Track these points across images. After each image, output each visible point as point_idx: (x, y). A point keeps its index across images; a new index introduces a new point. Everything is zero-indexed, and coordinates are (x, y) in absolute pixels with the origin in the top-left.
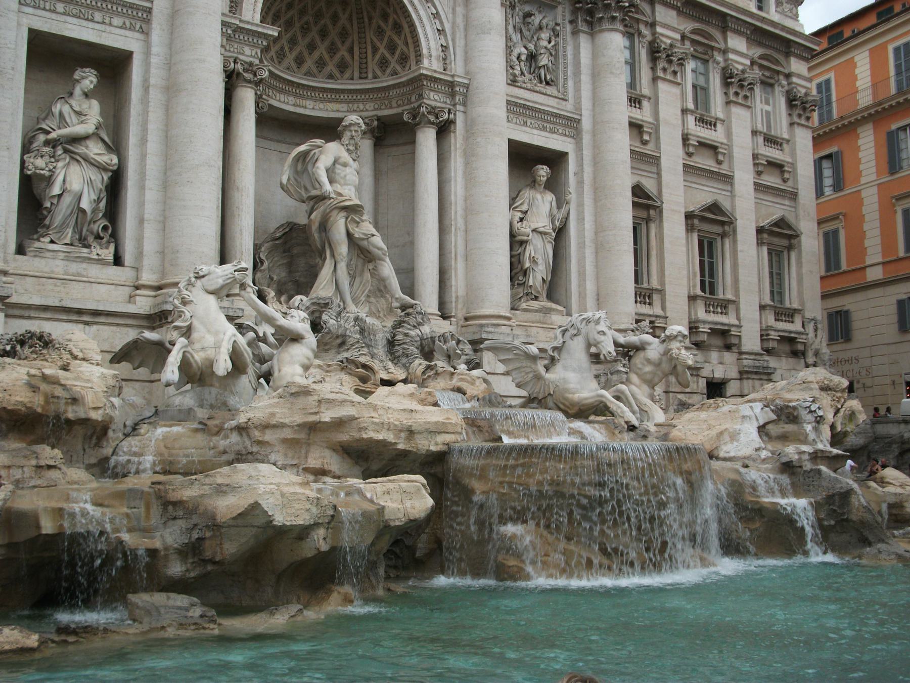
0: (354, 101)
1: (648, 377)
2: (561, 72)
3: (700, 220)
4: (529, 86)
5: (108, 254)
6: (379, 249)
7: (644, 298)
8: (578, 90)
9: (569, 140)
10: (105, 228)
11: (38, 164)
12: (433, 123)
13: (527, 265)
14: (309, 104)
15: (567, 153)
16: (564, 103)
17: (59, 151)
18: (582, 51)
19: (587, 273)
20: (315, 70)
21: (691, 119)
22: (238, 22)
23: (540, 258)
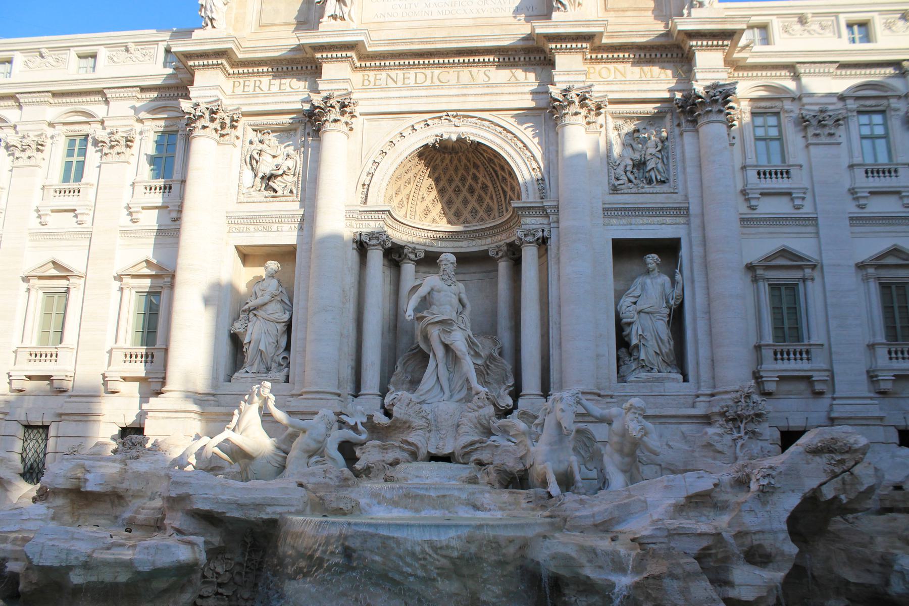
2: (671, 169)
3: (876, 269)
5: (281, 376)
6: (461, 351)
7: (801, 354)
8: (686, 182)
9: (681, 226)
10: (284, 358)
11: (238, 327)
12: (530, 243)
13: (634, 341)
14: (463, 244)
17: (251, 315)
20: (470, 218)
21: (860, 172)
23: (649, 334)
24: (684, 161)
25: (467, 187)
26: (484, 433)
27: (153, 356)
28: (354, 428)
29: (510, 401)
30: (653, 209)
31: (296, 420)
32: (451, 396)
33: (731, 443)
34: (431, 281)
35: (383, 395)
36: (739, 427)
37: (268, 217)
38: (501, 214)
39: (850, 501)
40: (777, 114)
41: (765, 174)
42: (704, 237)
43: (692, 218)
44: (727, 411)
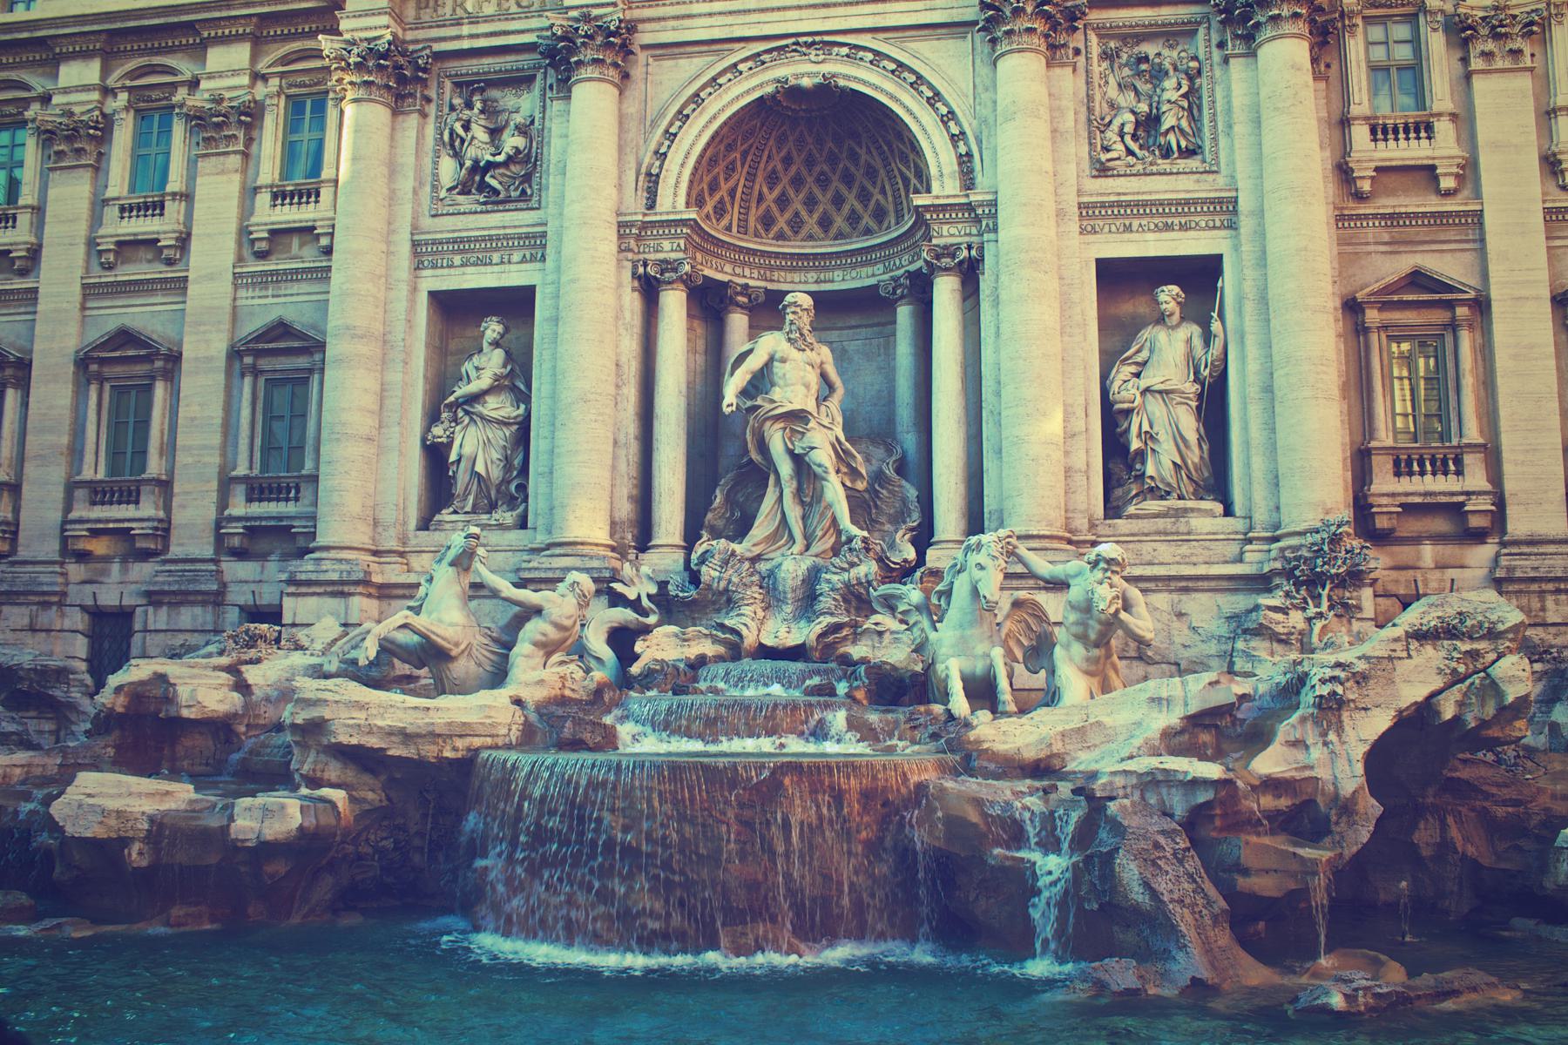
0: (889, 257)
1: (1074, 629)
4: (1140, 167)
6: (820, 466)
7: (1445, 462)
8: (1232, 148)
12: (946, 269)
13: (1135, 444)
15: (1218, 259)
16: (1210, 177)
17: (460, 414)
18: (1234, 87)
19: (1254, 443)
20: (846, 229)
22: (640, 217)
24: (1229, 111)
25: (838, 172)
26: (858, 609)
27: (298, 491)
28: (636, 605)
29: (910, 553)
30: (1170, 203)
31: (526, 595)
32: (807, 548)
33: (1301, 625)
34: (771, 342)
35: (689, 547)
36: (1320, 595)
37: (483, 239)
38: (899, 218)
39: (1484, 724)
40: (1412, 19)
41: (1385, 132)
42: (1264, 252)
43: (1242, 218)
44: (1296, 567)
